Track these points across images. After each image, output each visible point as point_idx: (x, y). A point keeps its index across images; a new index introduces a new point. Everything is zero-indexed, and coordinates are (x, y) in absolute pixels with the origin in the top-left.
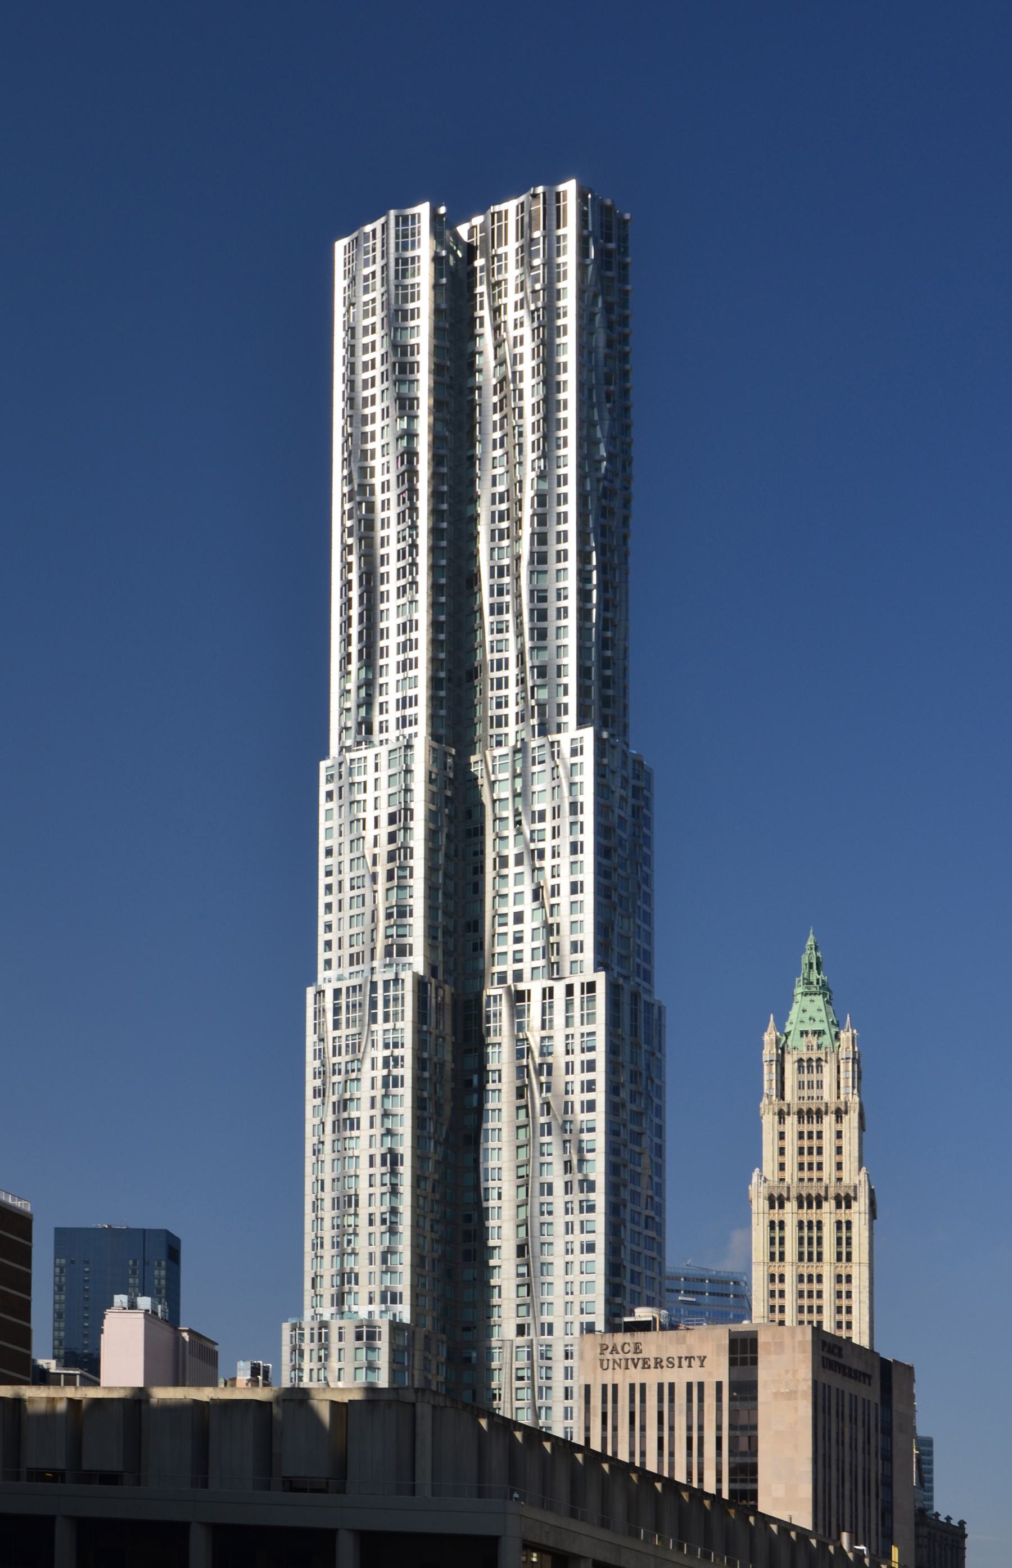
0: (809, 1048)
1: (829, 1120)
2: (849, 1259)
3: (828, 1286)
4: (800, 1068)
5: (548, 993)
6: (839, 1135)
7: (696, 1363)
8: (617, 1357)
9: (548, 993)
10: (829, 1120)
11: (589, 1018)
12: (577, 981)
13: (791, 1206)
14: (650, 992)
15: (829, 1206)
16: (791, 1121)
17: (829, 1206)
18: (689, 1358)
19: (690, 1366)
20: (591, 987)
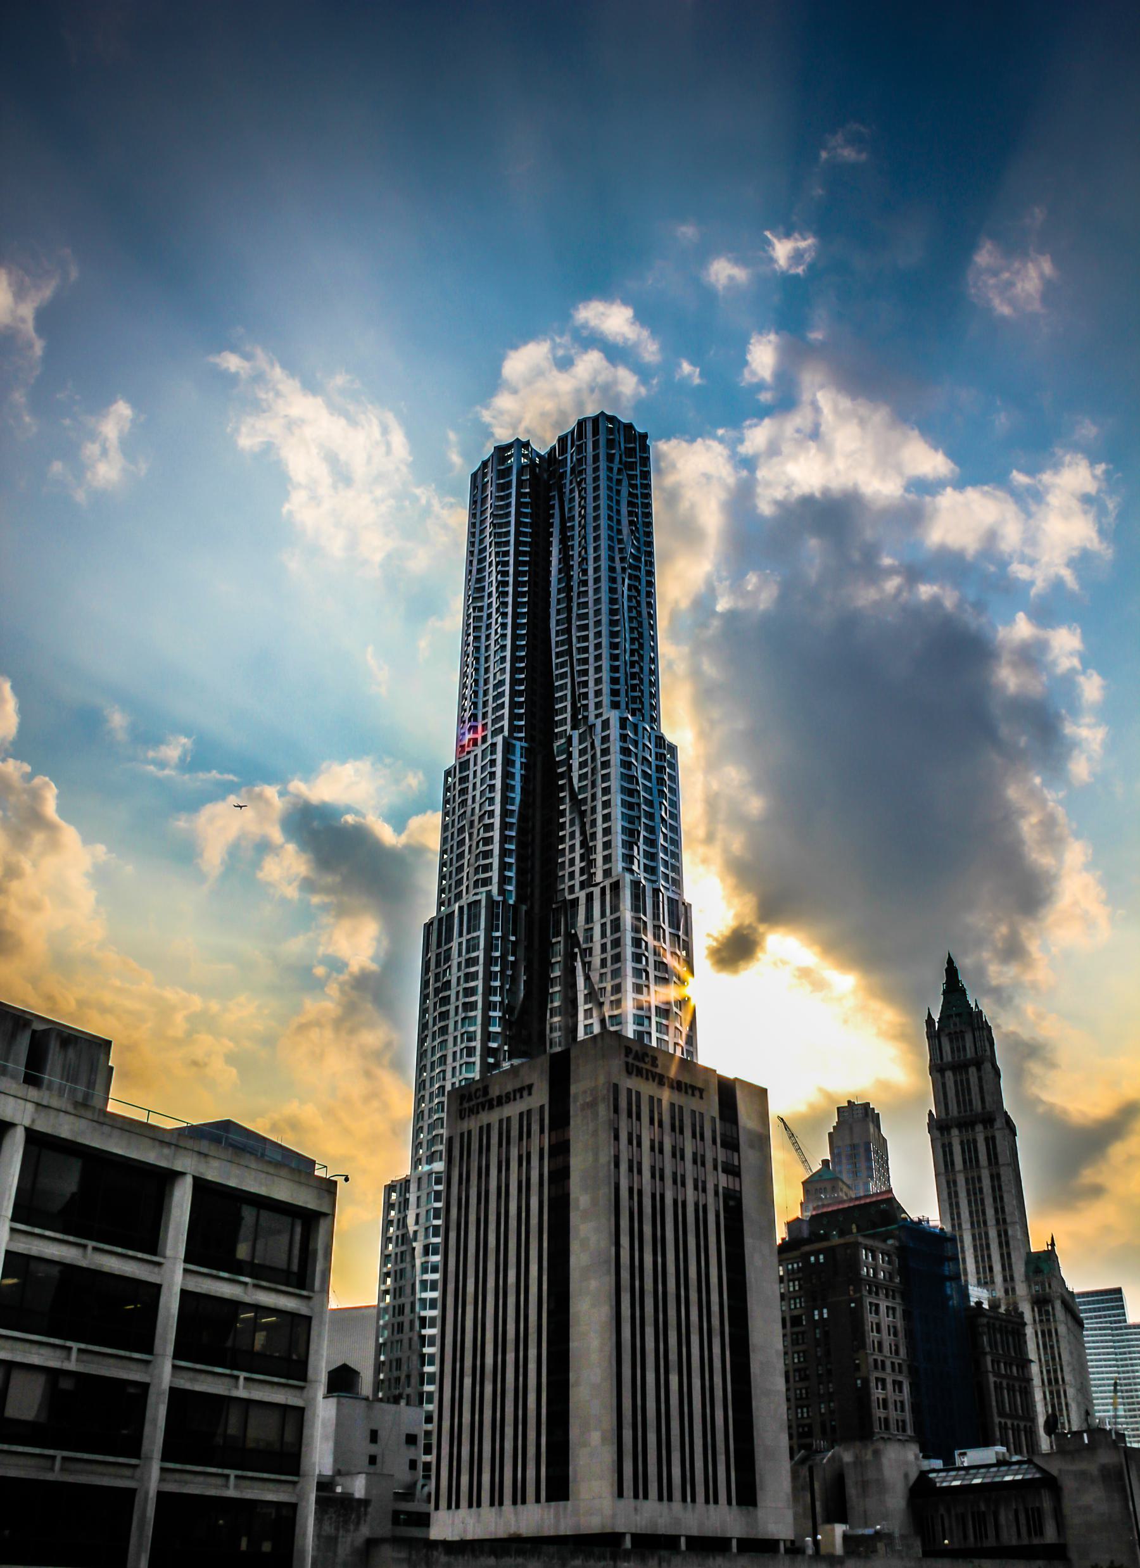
0: (955, 1025)
1: (972, 1070)
2: (997, 1163)
3: (986, 1183)
4: (951, 1041)
5: (590, 897)
6: (980, 1079)
7: (525, 1093)
8: (472, 1103)
9: (590, 897)
10: (972, 1070)
11: (615, 908)
12: (607, 883)
13: (955, 1132)
14: (680, 894)
15: (979, 1128)
16: (949, 1074)
17: (979, 1128)
18: (521, 1090)
19: (521, 1097)
20: (616, 887)
